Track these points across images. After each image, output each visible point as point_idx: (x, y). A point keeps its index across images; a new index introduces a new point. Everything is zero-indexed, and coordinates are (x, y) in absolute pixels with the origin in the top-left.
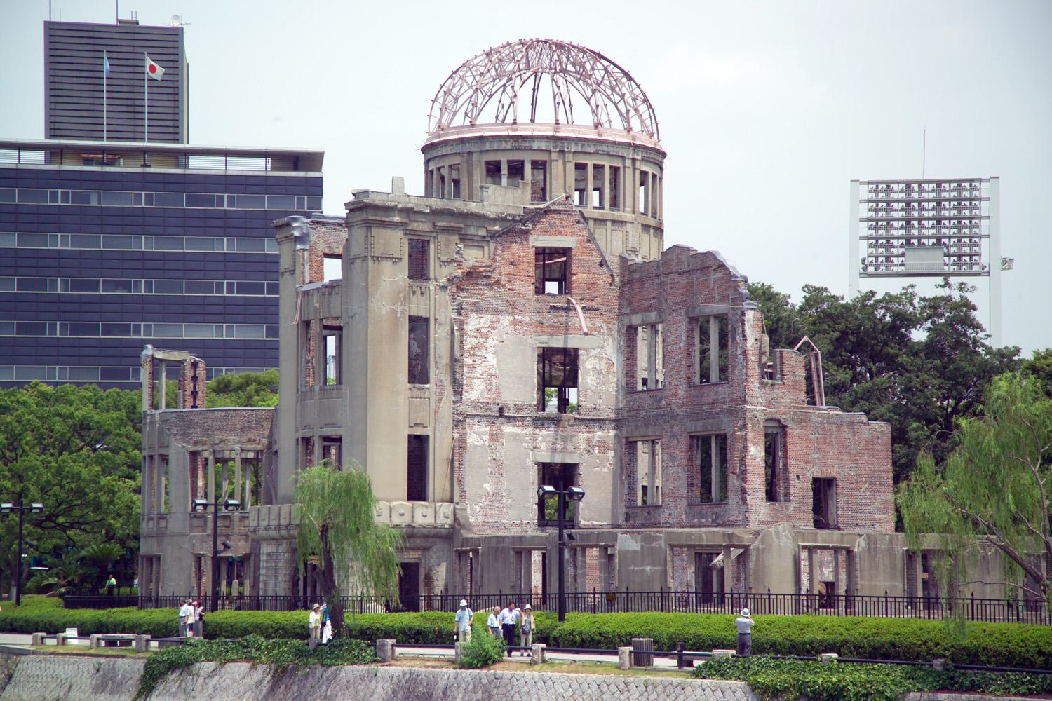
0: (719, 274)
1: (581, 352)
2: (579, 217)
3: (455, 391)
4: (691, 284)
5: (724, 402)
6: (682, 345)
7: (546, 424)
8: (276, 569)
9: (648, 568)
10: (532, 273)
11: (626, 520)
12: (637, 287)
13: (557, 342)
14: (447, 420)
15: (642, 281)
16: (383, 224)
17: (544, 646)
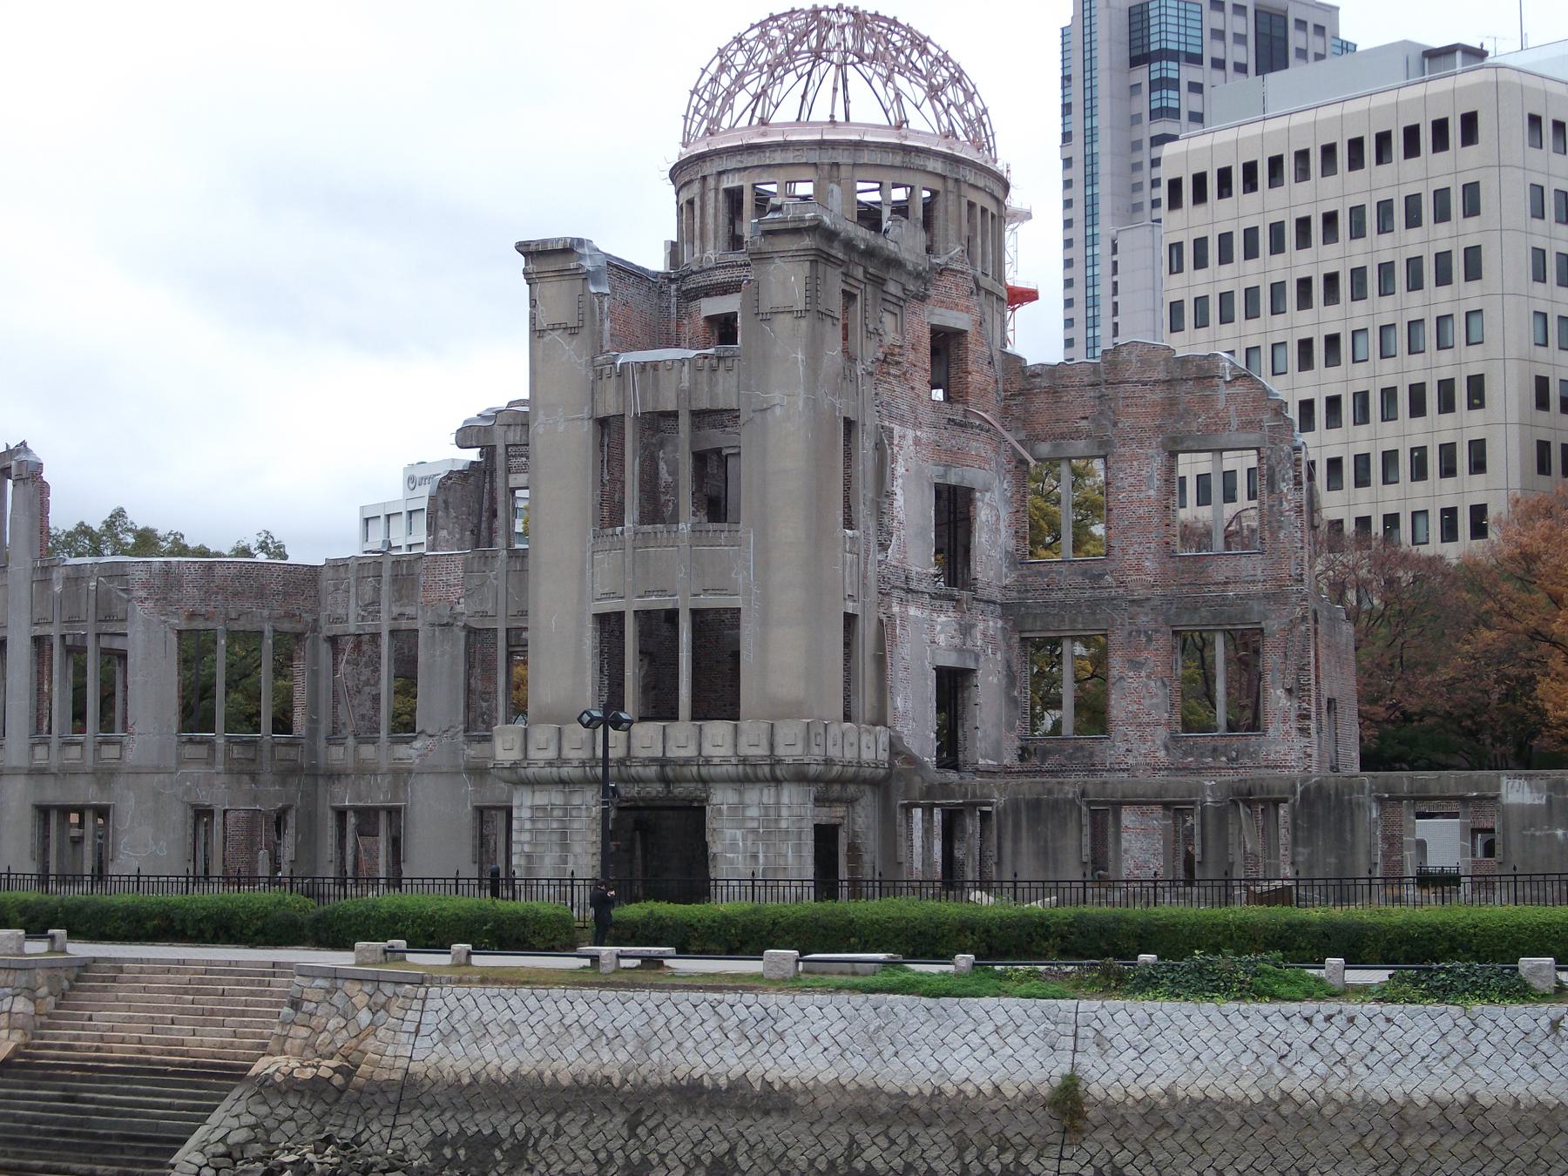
0: (1240, 388)
1: (978, 495)
2: (972, 285)
3: (881, 545)
4: (1172, 402)
5: (1254, 582)
6: (1152, 492)
7: (945, 604)
8: (564, 834)
9: (1560, 832)
10: (928, 366)
11: (1022, 758)
12: (1040, 402)
13: (953, 479)
14: (873, 590)
15: (1054, 392)
16: (829, 259)
17: (469, 947)
